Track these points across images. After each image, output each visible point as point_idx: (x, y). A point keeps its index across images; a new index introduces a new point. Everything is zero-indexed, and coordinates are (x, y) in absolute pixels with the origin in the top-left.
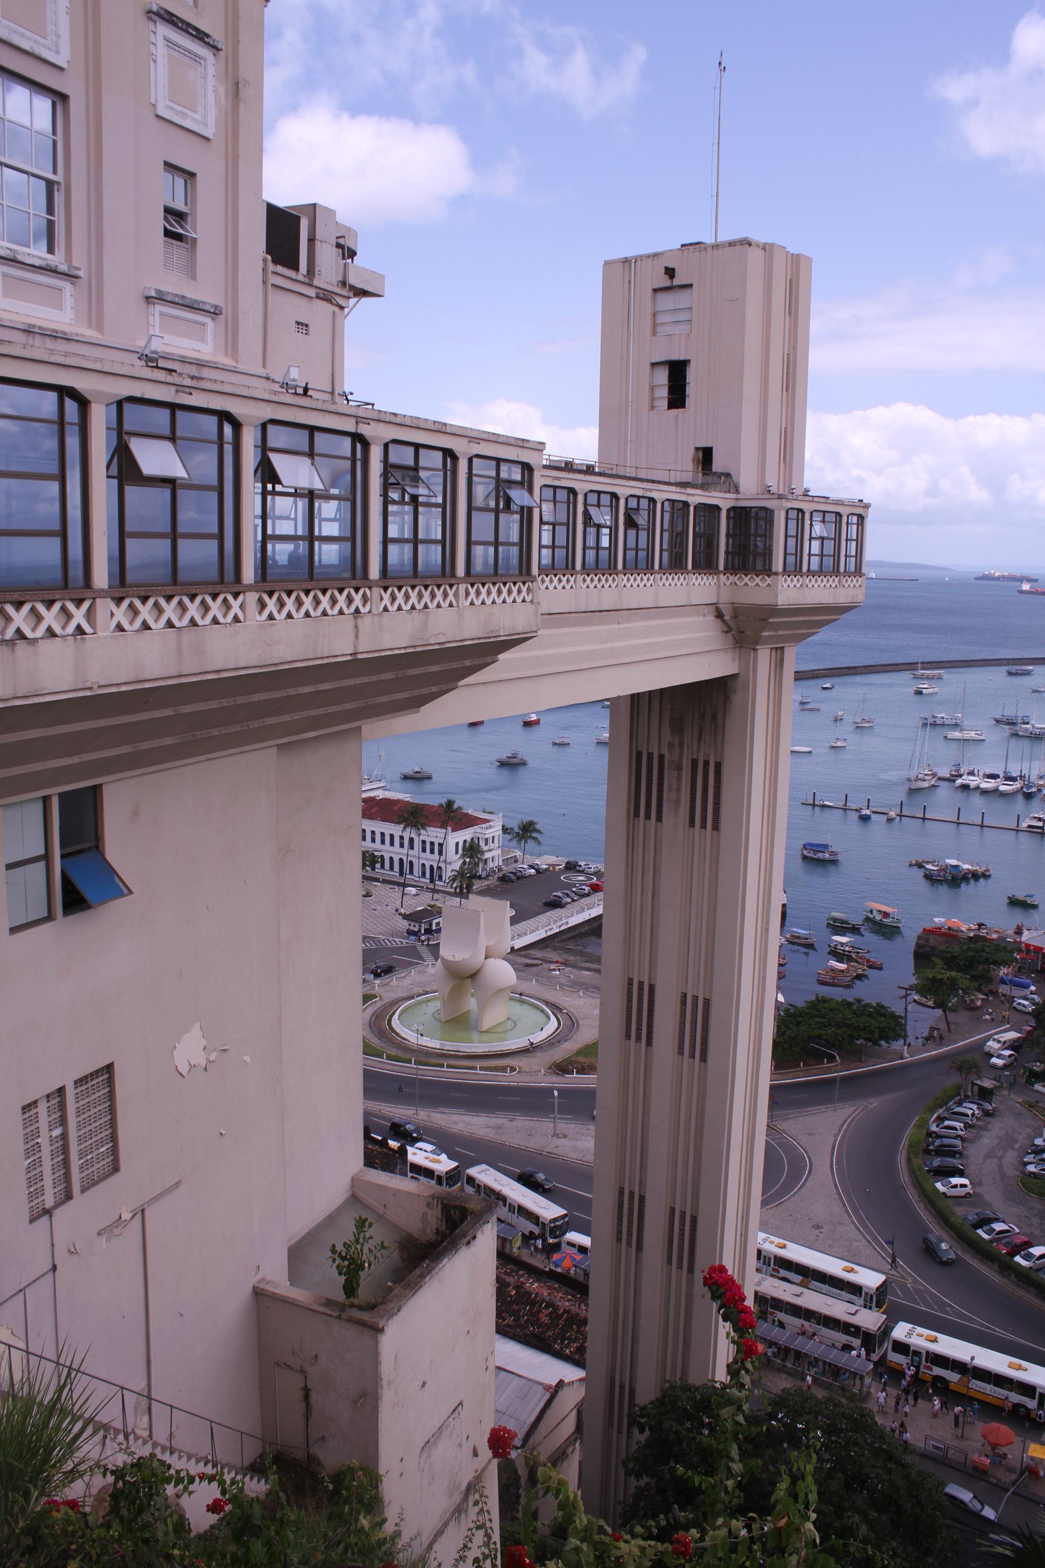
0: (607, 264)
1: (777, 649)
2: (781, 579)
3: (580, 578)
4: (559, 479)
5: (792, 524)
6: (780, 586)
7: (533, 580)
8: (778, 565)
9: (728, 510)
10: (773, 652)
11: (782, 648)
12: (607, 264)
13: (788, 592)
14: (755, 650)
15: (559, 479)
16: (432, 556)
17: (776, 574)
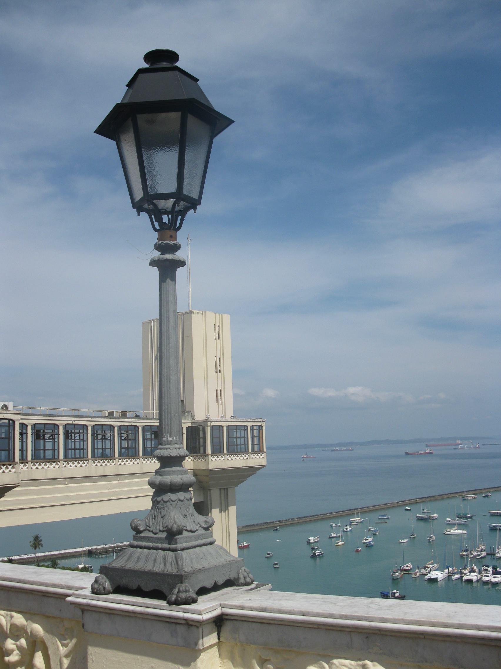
0: (143, 323)
1: (224, 489)
2: (210, 458)
3: (91, 462)
4: (75, 421)
5: (216, 433)
6: (210, 460)
7: (16, 463)
8: (209, 451)
9: (187, 428)
10: (223, 491)
11: (227, 488)
12: (143, 323)
13: (215, 462)
14: (210, 490)
15: (75, 421)
16: (82, 456)
17: (208, 455)
